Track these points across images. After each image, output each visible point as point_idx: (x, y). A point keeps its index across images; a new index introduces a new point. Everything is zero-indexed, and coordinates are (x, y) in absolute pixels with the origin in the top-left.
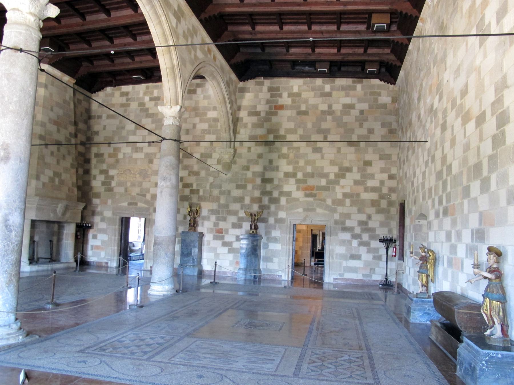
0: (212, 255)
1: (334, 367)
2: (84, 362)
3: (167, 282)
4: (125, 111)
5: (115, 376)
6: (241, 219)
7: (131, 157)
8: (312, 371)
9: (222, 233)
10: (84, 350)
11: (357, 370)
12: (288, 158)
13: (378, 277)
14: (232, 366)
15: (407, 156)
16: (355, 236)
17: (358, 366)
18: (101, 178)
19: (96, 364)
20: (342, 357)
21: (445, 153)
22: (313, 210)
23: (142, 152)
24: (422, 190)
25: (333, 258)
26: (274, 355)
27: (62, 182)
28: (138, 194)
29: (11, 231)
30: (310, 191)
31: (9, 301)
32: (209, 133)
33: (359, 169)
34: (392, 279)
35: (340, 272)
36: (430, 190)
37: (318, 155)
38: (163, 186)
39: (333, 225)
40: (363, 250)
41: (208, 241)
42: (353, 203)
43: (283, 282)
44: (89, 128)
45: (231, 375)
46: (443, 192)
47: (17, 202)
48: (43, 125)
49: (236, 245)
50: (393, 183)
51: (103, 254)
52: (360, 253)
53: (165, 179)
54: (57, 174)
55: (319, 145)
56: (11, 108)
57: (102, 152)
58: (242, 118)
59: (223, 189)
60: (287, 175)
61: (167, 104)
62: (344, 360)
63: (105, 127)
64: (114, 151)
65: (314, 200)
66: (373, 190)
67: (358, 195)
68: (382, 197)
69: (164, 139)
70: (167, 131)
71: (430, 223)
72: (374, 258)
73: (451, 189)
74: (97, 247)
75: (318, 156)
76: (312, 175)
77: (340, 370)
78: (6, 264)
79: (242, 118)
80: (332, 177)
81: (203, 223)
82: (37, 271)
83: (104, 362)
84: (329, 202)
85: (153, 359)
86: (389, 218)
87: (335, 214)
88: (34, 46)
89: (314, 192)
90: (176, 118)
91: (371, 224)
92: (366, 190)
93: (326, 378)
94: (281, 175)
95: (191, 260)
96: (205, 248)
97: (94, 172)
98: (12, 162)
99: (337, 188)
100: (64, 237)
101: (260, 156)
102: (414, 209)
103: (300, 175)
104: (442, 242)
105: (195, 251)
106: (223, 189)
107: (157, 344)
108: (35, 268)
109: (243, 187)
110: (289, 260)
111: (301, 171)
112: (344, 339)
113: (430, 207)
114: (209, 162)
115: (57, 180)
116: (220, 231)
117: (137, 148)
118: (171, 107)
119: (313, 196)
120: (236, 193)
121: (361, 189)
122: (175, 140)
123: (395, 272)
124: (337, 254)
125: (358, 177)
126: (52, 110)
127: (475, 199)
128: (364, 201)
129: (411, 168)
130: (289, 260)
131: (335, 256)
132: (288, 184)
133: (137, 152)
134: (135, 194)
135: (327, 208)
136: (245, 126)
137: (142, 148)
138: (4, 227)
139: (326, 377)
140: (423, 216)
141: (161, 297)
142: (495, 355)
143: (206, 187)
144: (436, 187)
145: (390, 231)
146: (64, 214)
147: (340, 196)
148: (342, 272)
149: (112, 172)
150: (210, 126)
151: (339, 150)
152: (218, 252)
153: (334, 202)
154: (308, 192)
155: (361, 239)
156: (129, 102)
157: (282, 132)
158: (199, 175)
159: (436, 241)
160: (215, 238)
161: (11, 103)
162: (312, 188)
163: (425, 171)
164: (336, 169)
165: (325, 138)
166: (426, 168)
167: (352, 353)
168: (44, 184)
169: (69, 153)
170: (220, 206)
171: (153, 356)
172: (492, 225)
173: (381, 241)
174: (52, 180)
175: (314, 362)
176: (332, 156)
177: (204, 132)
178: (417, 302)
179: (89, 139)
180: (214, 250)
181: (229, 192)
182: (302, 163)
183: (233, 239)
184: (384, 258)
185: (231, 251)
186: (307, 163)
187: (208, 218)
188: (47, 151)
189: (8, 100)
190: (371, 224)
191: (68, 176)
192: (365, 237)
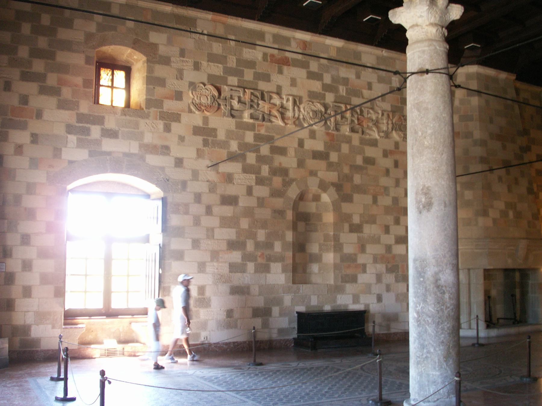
27: (518, 215)
29: (444, 293)
31: (448, 379)
47: (447, 256)
48: (483, 143)
54: (510, 205)
56: (426, 143)
78: (442, 333)
82: (498, 337)
88: (440, 62)
98: (435, 208)
100: (530, 289)
108: (494, 332)
115: (511, 214)
138: (435, 288)
146: (526, 258)
161: (425, 138)
168: (495, 221)
174: (504, 214)
189: (422, 134)
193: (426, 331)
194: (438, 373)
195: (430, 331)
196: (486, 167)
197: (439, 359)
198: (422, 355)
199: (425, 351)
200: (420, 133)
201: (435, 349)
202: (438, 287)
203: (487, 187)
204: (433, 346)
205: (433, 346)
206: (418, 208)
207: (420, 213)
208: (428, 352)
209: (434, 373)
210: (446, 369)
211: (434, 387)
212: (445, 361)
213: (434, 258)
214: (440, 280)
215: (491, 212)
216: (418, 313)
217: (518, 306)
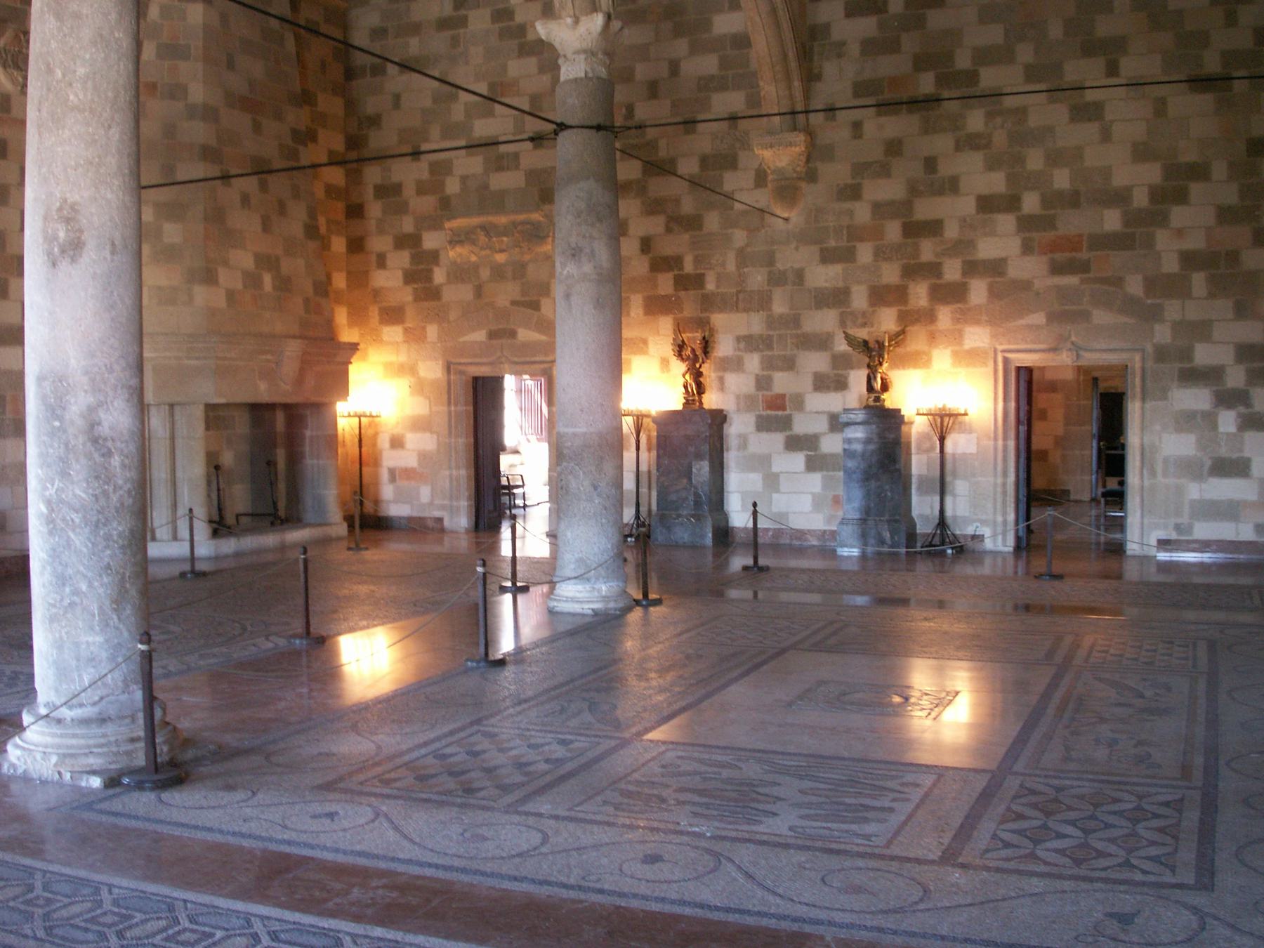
2: (331, 816)
3: (602, 571)
4: (455, 41)
5: (408, 857)
7: (486, 187)
8: (1007, 845)
9: (784, 409)
10: (335, 782)
11: (1153, 843)
12: (988, 146)
14: (754, 828)
16: (1226, 399)
17: (1161, 830)
18: (400, 260)
19: (362, 821)
20: (1116, 801)
22: (1084, 316)
23: (517, 167)
25: (1153, 474)
27: (284, 284)
28: (514, 303)
29: (108, 454)
30: (1067, 255)
31: (124, 651)
32: (723, 87)
35: (1179, 521)
37: (1092, 129)
38: (569, 276)
41: (740, 436)
42: (1217, 288)
43: (988, 561)
44: (351, 105)
45: (744, 854)
47: (117, 368)
48: (209, 114)
49: (832, 444)
51: (425, 493)
52: (1247, 454)
53: (575, 254)
54: (267, 262)
57: (395, 178)
58: (827, 26)
59: (780, 266)
60: (987, 204)
61: (564, 14)
63: (397, 98)
64: (432, 173)
65: (1082, 281)
67: (1233, 257)
69: (562, 127)
70: (570, 101)
74: (408, 473)
75: (1090, 130)
76: (1073, 200)
77: (1100, 845)
79: (827, 26)
80: (1141, 199)
82: (238, 555)
83: (386, 816)
84: (1134, 286)
85: (530, 807)
87: (1157, 327)
89: (1084, 255)
90: (593, 54)
93: (1042, 868)
94: (966, 205)
95: (691, 498)
97: (379, 243)
99: (1163, 239)
100: (307, 449)
101: (894, 148)
103: (1031, 203)
105: (702, 470)
106: (780, 266)
107: (547, 761)
108: (229, 546)
109: (847, 256)
110: (1004, 485)
111: (1032, 189)
112: (1140, 743)
115: (267, 279)
116: (777, 403)
117: (500, 157)
118: (577, 21)
119: (1081, 268)
120: (823, 276)
122: (599, 128)
125: (1230, 195)
126: (231, 65)
130: (1004, 485)
131: (1159, 468)
132: (993, 233)
133: (500, 169)
134: (507, 304)
135: (1130, 306)
136: (839, 49)
137: (516, 156)
138: (89, 444)
139: (1046, 863)
141: (588, 619)
143: (723, 265)
146: (300, 381)
147: (1171, 265)
148: (1184, 520)
149: (431, 241)
150: (724, 64)
152: (775, 469)
154: (1058, 256)
155: (1248, 404)
156: (463, 12)
157: (963, 61)
158: (700, 228)
160: (764, 425)
162: (1073, 243)
164: (1152, 173)
165: (1112, 70)
167: (1153, 790)
168: (231, 295)
169: (296, 195)
170: (771, 322)
174: (252, 280)
175: (1020, 817)
177: (708, 85)
179: (354, 142)
180: (761, 463)
181: (800, 275)
182: (1035, 161)
183: (821, 425)
185: (813, 465)
186: (1055, 159)
188: (230, 194)
191: (301, 262)
193: (69, 544)
194: (99, 639)
195: (77, 543)
196: (215, 171)
197: (100, 608)
198: (62, 600)
199: (67, 590)
200: (59, 74)
201: (90, 585)
202: (95, 441)
203: (216, 216)
204: (85, 576)
205: (85, 576)
206: (49, 253)
207: (54, 265)
208: (76, 592)
209: (90, 639)
210: (117, 628)
211: (92, 670)
212: (115, 610)
213: (86, 373)
214: (99, 424)
215: (223, 274)
216: (48, 503)
217: (282, 486)
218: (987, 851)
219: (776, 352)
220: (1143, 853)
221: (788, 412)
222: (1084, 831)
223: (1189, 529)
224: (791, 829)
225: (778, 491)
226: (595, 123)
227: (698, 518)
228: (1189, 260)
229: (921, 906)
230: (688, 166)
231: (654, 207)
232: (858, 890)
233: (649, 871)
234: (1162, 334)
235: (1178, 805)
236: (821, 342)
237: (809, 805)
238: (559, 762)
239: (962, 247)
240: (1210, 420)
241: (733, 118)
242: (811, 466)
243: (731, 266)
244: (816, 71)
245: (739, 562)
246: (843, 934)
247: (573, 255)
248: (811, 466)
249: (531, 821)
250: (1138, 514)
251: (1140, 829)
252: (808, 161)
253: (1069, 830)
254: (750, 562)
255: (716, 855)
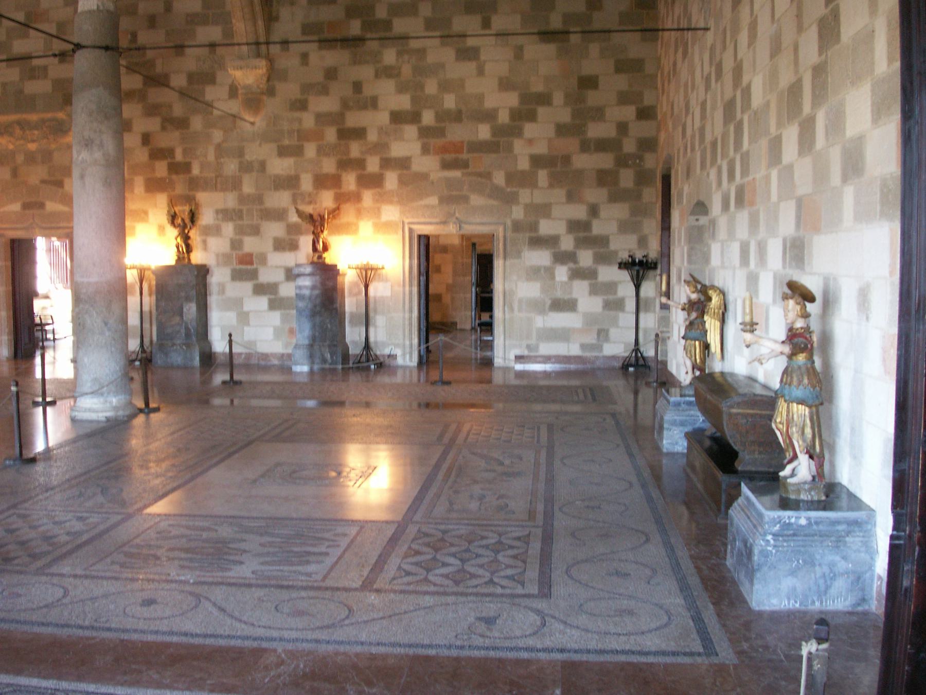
0: (230, 318)
1: (458, 562)
6: (294, 230)
8: (408, 574)
9: (251, 263)
11: (508, 567)
12: (398, 75)
13: (617, 346)
15: (675, 64)
16: (562, 258)
17: (515, 557)
20: (483, 538)
21: (739, 57)
22: (466, 199)
24: (700, 145)
25: (512, 309)
26: (327, 543)
30: (453, 155)
33: (567, 96)
34: (649, 351)
35: (529, 342)
36: (714, 144)
39: (509, 234)
40: (580, 289)
42: (555, 181)
43: (400, 373)
45: (218, 594)
46: (736, 151)
49: (287, 290)
50: (640, 129)
52: (574, 295)
53: (88, 144)
55: (471, 42)
59: (248, 157)
60: (397, 118)
62: (486, 547)
65: (463, 175)
66: (602, 145)
67: (567, 159)
68: (622, 161)
71: (713, 223)
72: (607, 305)
73: (750, 144)
75: (468, 68)
76: (457, 117)
77: (472, 570)
80: (504, 117)
81: (204, 242)
84: (499, 178)
86: (639, 211)
87: (514, 208)
89: (465, 156)
91: (597, 228)
92: (585, 147)
93: (432, 588)
94: (383, 118)
95: (183, 331)
96: (213, 300)
99: (519, 147)
101: (331, 74)
102: (686, 189)
103: (428, 118)
104: (734, 268)
106: (248, 157)
107: (68, 534)
109: (296, 151)
110: (410, 318)
111: (430, 108)
112: (501, 497)
113: (714, 186)
114: (211, 93)
116: (247, 259)
119: (463, 165)
120: (280, 166)
121: (570, 145)
122: (107, 48)
123: (653, 337)
124: (520, 301)
125: (565, 116)
127: (790, 167)
128: (580, 173)
129: (682, 90)
130: (410, 318)
139: (435, 585)
140: (701, 208)
141: (102, 425)
142: (793, 520)
143: (206, 156)
144: (725, 136)
145: (643, 242)
147: (524, 164)
148: (533, 342)
151: (519, 53)
152: (246, 309)
153: (510, 178)
155: (575, 262)
157: (381, 13)
159: (723, 267)
160: (237, 276)
162: (457, 147)
163: (706, 100)
164: (512, 99)
165: (486, 24)
166: (706, 93)
167: (509, 529)
170: (242, 199)
171: (50, 565)
172: (817, 230)
173: (623, 265)
175: (417, 553)
176: (503, 69)
178: (678, 404)
180: (236, 304)
181: (263, 165)
182: (431, 87)
183: (279, 276)
184: (631, 305)
185: (275, 305)
186: (445, 86)
187: (215, 230)
190: (597, 228)
192: (586, 258)
218: (394, 579)
219: (246, 222)
220: (502, 574)
221: (255, 266)
222: (461, 560)
223: (536, 348)
224: (253, 572)
225: (248, 324)
226: (104, 45)
227: (188, 346)
228: (537, 161)
229: (347, 622)
230: (179, 81)
231: (152, 110)
232: (300, 613)
233: (146, 612)
234: (518, 213)
235: (526, 540)
236: (279, 215)
237: (268, 554)
238: (78, 534)
239: (380, 147)
240: (550, 272)
241: (213, 46)
242: (273, 306)
243: (211, 157)
244: (274, 14)
245: (220, 377)
246: (290, 647)
247: (87, 145)
248: (273, 306)
249: (55, 580)
250: (502, 337)
251: (500, 557)
252: (268, 80)
253: (451, 560)
254: (227, 377)
255: (198, 597)
